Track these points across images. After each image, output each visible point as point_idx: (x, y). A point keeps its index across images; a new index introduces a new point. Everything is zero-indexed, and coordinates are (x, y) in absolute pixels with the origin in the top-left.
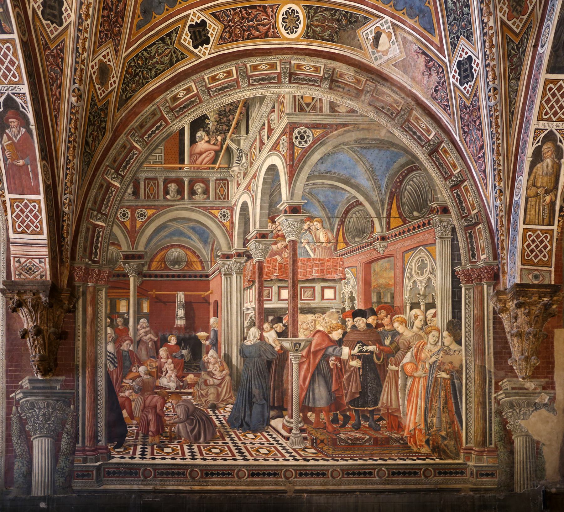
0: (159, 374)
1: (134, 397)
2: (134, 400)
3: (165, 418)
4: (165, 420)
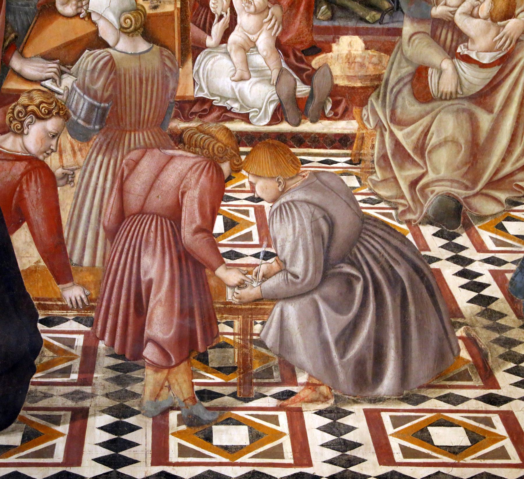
0: (195, 31)
1: (68, 159)
2: (68, 178)
3: (221, 272)
4: (222, 285)
